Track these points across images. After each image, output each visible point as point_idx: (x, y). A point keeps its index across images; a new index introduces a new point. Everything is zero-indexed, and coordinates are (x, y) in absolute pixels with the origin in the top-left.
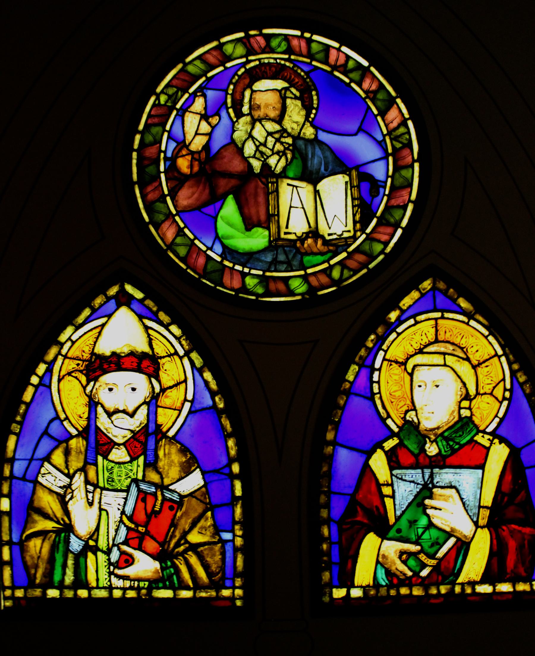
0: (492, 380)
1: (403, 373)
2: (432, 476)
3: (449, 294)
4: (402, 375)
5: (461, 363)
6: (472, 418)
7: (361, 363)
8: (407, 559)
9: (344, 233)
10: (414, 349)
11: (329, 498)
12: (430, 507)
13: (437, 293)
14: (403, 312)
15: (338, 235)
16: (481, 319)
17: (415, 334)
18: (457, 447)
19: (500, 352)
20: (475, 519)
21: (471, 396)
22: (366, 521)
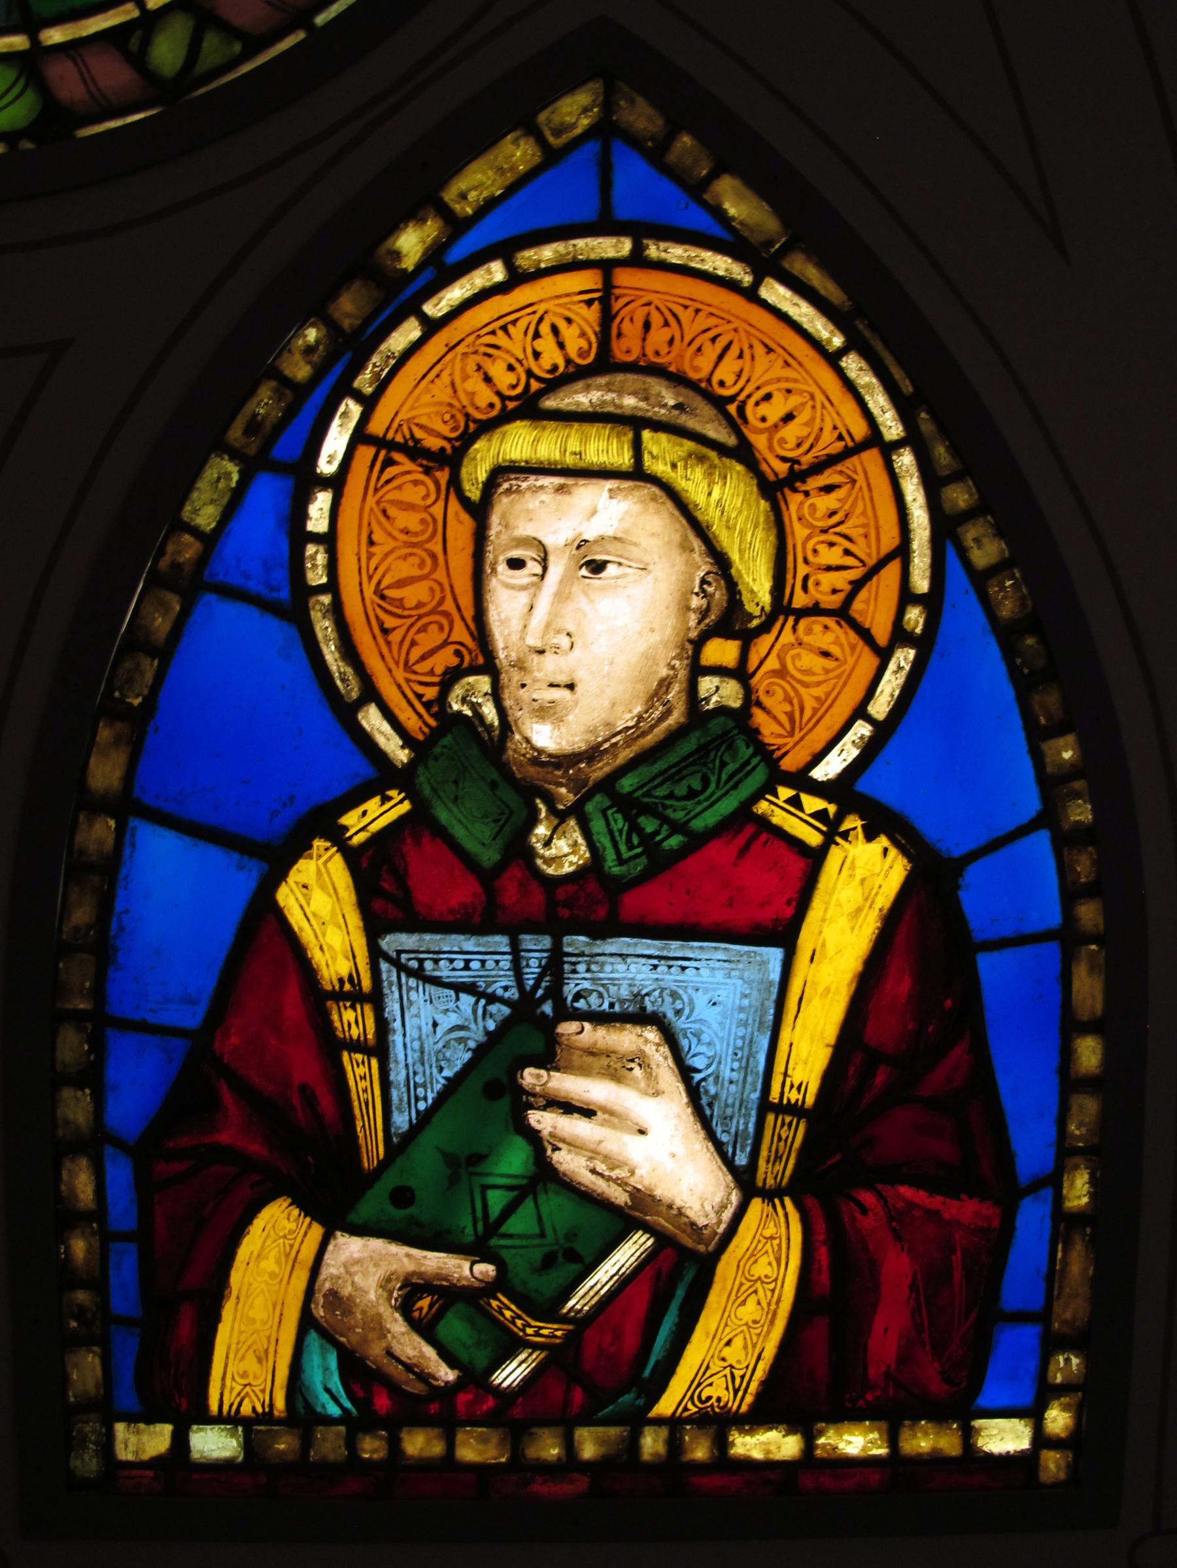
0: (847, 552)
1: (441, 504)
2: (555, 965)
3: (672, 157)
4: (438, 510)
5: (713, 467)
6: (750, 716)
7: (252, 450)
8: (439, 1316)
10: (499, 394)
11: (97, 1044)
12: (542, 1102)
13: (618, 148)
14: (456, 226)
16: (813, 275)
17: (504, 328)
18: (674, 842)
19: (892, 428)
20: (741, 1159)
21: (751, 617)
22: (255, 1148)
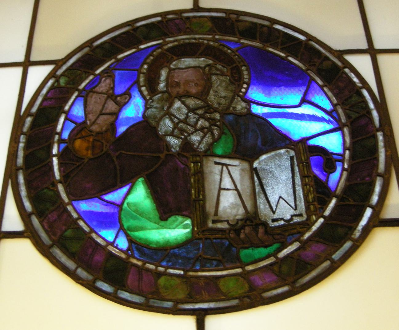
9: (294, 217)
15: (285, 221)
